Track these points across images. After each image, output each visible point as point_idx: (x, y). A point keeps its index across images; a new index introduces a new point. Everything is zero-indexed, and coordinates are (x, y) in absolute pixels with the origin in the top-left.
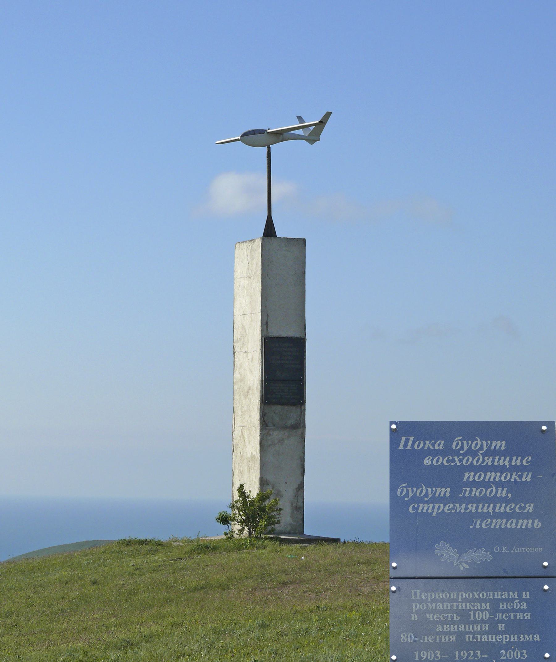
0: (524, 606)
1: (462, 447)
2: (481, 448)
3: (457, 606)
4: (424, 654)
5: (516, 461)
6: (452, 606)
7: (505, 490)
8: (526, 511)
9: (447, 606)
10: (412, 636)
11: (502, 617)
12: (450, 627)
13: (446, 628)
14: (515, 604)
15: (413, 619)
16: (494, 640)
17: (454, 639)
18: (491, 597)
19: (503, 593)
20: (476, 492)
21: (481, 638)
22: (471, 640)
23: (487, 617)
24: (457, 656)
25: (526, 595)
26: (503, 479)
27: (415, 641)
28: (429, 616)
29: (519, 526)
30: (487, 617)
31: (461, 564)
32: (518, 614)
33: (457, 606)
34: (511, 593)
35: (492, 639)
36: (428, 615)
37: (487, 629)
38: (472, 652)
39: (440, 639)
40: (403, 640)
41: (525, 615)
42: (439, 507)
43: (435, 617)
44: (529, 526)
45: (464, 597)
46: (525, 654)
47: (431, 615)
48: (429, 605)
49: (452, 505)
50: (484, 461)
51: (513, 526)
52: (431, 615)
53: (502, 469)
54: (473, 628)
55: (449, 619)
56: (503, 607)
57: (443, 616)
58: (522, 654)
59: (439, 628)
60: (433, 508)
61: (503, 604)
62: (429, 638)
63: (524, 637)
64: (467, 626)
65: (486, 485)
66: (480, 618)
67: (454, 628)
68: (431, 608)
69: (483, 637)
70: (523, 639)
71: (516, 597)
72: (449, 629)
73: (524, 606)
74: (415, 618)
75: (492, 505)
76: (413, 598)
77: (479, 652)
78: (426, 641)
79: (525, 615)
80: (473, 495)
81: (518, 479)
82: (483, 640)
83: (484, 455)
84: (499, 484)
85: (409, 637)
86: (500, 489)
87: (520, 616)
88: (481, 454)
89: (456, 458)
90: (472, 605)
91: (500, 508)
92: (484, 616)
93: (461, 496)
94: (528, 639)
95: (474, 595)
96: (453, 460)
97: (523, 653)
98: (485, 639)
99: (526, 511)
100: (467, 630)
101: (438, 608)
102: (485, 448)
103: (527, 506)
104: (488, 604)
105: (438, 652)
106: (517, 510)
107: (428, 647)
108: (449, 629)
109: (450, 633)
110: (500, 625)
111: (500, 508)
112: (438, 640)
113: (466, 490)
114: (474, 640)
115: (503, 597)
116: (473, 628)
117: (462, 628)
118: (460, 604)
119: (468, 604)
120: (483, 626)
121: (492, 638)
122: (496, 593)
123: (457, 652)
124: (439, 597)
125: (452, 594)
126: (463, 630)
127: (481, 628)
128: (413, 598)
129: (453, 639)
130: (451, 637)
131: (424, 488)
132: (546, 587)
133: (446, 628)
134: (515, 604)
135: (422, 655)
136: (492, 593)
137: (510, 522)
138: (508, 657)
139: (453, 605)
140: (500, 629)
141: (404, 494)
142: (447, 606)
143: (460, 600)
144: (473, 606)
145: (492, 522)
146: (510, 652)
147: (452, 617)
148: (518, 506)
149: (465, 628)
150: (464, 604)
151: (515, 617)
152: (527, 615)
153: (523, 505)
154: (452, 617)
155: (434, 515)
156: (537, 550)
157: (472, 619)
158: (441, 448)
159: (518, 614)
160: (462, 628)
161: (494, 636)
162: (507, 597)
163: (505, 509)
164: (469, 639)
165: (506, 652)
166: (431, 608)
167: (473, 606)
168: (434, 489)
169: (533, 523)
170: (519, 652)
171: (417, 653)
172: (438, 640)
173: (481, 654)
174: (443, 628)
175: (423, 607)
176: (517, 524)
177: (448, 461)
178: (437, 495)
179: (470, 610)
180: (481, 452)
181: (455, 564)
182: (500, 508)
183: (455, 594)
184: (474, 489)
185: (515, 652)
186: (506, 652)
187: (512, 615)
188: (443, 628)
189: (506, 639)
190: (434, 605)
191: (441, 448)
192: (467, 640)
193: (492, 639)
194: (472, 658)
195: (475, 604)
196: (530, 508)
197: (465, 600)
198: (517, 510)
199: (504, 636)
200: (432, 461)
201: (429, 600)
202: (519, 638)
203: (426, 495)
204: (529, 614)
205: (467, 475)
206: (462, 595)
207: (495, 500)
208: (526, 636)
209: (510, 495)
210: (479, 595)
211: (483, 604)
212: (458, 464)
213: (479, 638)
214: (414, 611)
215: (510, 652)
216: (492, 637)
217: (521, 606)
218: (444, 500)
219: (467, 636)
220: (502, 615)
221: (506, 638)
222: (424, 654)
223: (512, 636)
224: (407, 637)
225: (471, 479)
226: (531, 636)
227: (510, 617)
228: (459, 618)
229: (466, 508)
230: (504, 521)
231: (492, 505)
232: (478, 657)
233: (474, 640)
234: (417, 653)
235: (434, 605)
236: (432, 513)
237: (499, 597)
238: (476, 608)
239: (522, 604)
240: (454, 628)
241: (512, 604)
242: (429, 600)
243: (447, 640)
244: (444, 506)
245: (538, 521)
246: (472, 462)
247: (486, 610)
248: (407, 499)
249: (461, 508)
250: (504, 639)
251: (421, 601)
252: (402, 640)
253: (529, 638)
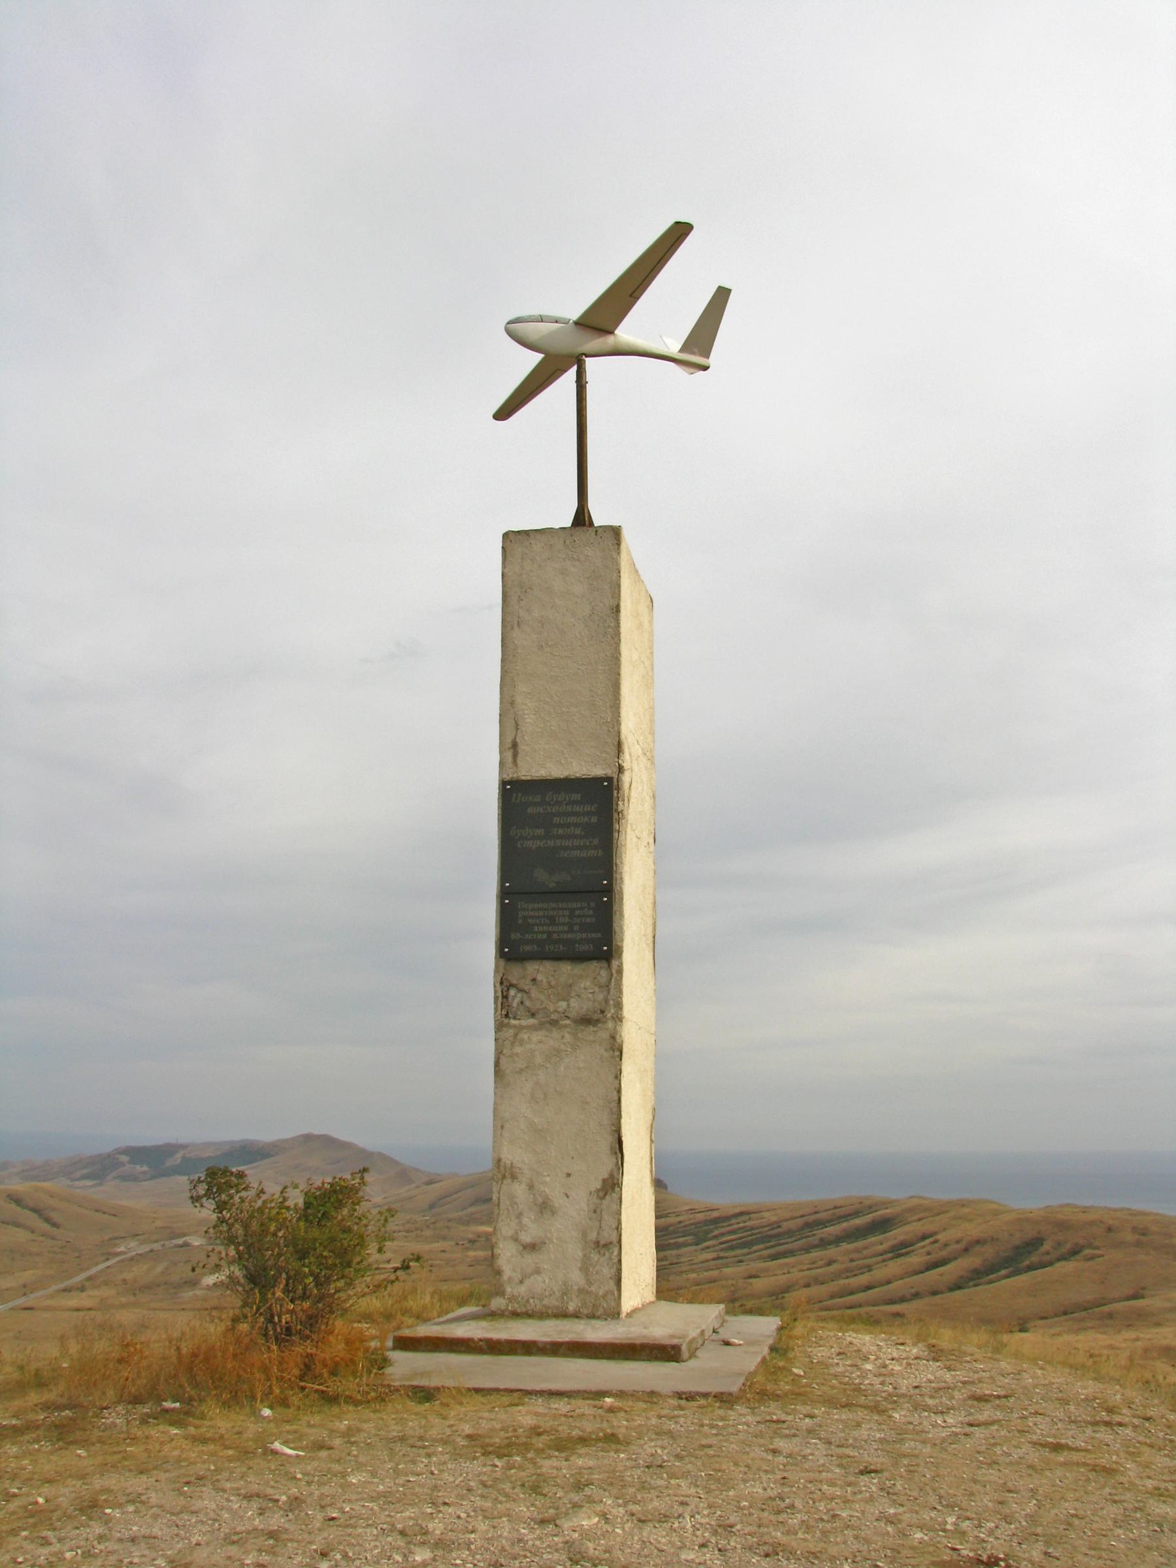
0: (591, 912)
5: (587, 808)
9: (541, 913)
13: (541, 929)
20: (561, 831)
53: (577, 814)
65: (568, 825)
67: (545, 928)
73: (591, 912)
84: (576, 825)
87: (588, 920)
91: (577, 842)
107: (528, 942)
109: (543, 932)
117: (550, 928)
121: (570, 936)
129: (545, 936)
133: (541, 929)
142: (541, 913)
160: (550, 928)
175: (526, 913)
182: (577, 842)
196: (596, 842)
197: (554, 909)
207: (575, 837)
218: (539, 838)
221: (579, 936)
240: (545, 928)
249: (551, 843)
251: (524, 910)
253: (594, 935)
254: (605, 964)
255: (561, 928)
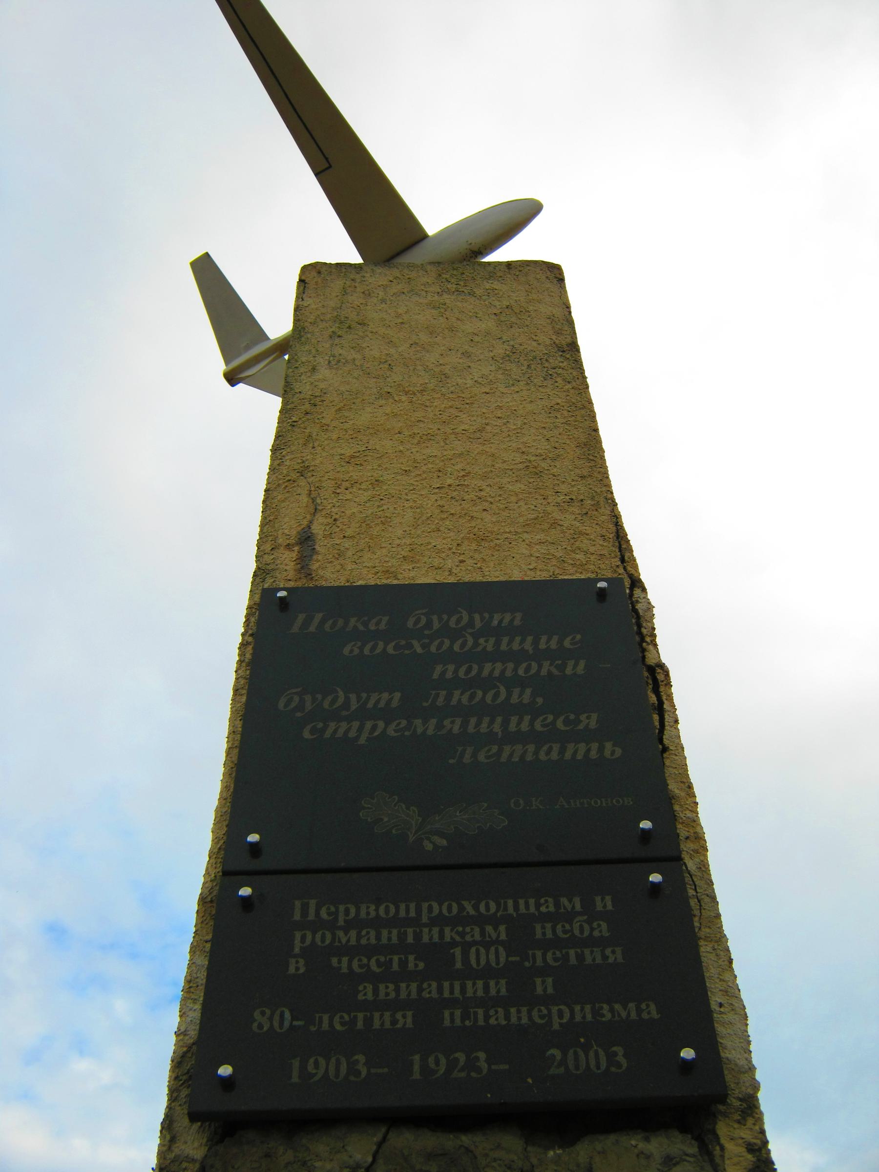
0: (603, 929)
1: (429, 625)
2: (471, 624)
3: (418, 936)
4: (316, 1065)
6: (402, 937)
7: (528, 691)
8: (581, 727)
10: (287, 1015)
11: (544, 959)
12: (397, 990)
13: (386, 991)
14: (576, 926)
15: (292, 970)
16: (525, 1020)
17: (409, 1020)
18: (511, 910)
19: (542, 901)
21: (487, 1017)
22: (458, 1022)
23: (502, 959)
24: (416, 1068)
25: (604, 903)
26: (521, 672)
27: (292, 1027)
28: (340, 962)
29: (568, 755)
30: (502, 959)
31: (428, 839)
32: (587, 952)
33: (418, 936)
34: (564, 901)
35: (519, 1018)
36: (334, 961)
37: (503, 991)
38: (461, 1057)
39: (368, 1021)
40: (260, 1026)
41: (608, 951)
42: (374, 728)
43: (355, 964)
44: (593, 754)
45: (436, 911)
46: (620, 1058)
47: (345, 960)
48: (341, 934)
49: (404, 723)
50: (476, 644)
51: (554, 756)
52: (345, 960)
54: (463, 990)
55: (395, 967)
56: (544, 934)
57: (377, 961)
58: (611, 1056)
59: (366, 992)
60: (360, 729)
61: (543, 928)
62: (337, 1019)
63: (612, 1010)
64: (446, 985)
66: (483, 962)
67: (409, 990)
68: (344, 940)
69: (492, 1012)
70: (609, 1016)
71: (578, 907)
72: (393, 995)
73: (603, 929)
74: (297, 969)
75: (499, 719)
76: (297, 916)
77: (482, 1055)
78: (325, 1026)
79: (608, 951)
80: (454, 701)
81: (555, 672)
82: (492, 1021)
83: (476, 636)
85: (277, 1018)
86: (516, 691)
88: (470, 634)
89: (415, 643)
90: (457, 933)
92: (492, 957)
93: (425, 704)
94: (624, 1014)
95: (462, 908)
96: (410, 646)
97: (615, 1054)
98: (498, 1018)
99: (581, 727)
100: (446, 994)
101: (364, 941)
102: (478, 624)
103: (583, 717)
104: (502, 928)
105: (361, 1058)
106: (560, 724)
108: (393, 995)
110: (538, 981)
111: (519, 724)
112: (360, 1025)
113: (438, 695)
114: (467, 1023)
115: (543, 909)
116: (463, 990)
117: (431, 990)
118: (426, 930)
119: (447, 930)
120: (492, 983)
121: (519, 1016)
122: (522, 902)
123: (417, 1058)
124: (368, 913)
125: (403, 907)
126: (435, 995)
127: (486, 988)
128: (297, 916)
129: (406, 1020)
130: (399, 1016)
131: (341, 694)
132: (655, 878)
133: (386, 991)
134: (576, 926)
135: (311, 1068)
136: (510, 903)
137: (545, 748)
138: (571, 1066)
139: (405, 933)
140: (539, 990)
141: (293, 705)
143: (425, 919)
144: (462, 935)
145: (500, 751)
146: (576, 1053)
147: (403, 964)
148: (562, 718)
149: (440, 989)
150: (435, 930)
151: (580, 957)
152: (613, 952)
153: (572, 717)
154: (403, 964)
155: (362, 741)
156: (618, 802)
157: (459, 965)
158: (382, 626)
159: (587, 952)
160: (431, 990)
161: (524, 1009)
162: (552, 909)
163: (532, 723)
164: (452, 1020)
165: (565, 1054)
166: (344, 940)
167: (462, 935)
168: (364, 695)
169: (601, 749)
170: (601, 1053)
171: (296, 1063)
172: (360, 1025)
173: (488, 1061)
174: (376, 991)
176: (562, 751)
177: (396, 648)
178: (370, 705)
179: (453, 944)
180: (470, 631)
181: (411, 838)
183: (412, 906)
184: (457, 693)
185: (592, 1054)
186: (565, 1054)
187: (572, 952)
188: (376, 991)
189: (561, 1015)
190: (353, 934)
191: (382, 626)
192: (447, 1022)
193: (519, 1018)
194: (463, 1074)
195: (468, 929)
196: (591, 721)
197: (439, 921)
198: (560, 724)
199: (554, 1010)
200: (361, 649)
201: (341, 922)
202: (596, 1013)
203: (346, 705)
204: (619, 950)
205: (439, 669)
206: (430, 909)
208: (617, 1006)
209: (540, 701)
210: (476, 907)
211: (489, 929)
212: (419, 650)
213: (481, 1017)
214: (297, 950)
215: (576, 1053)
216: (519, 1012)
217: (592, 929)
219: (447, 1014)
220: (544, 956)
222: (316, 1065)
223: (577, 1008)
224: (271, 1019)
225: (449, 675)
226: (632, 1005)
227: (566, 957)
228: (421, 965)
229: (439, 726)
230: (531, 748)
231: (499, 719)
232: (479, 1070)
233: (467, 1023)
234: (296, 1063)
235: (353, 934)
236: (357, 738)
237: (532, 909)
238: (468, 938)
239: (595, 925)
240: (409, 990)
241: (568, 927)
242: (341, 922)
243: (387, 1025)
244: (387, 724)
245: (614, 745)
246: (451, 647)
247: (497, 942)
248: (299, 714)
250: (556, 1020)
252: (255, 1025)
254: (678, 1144)
255: (475, 989)
